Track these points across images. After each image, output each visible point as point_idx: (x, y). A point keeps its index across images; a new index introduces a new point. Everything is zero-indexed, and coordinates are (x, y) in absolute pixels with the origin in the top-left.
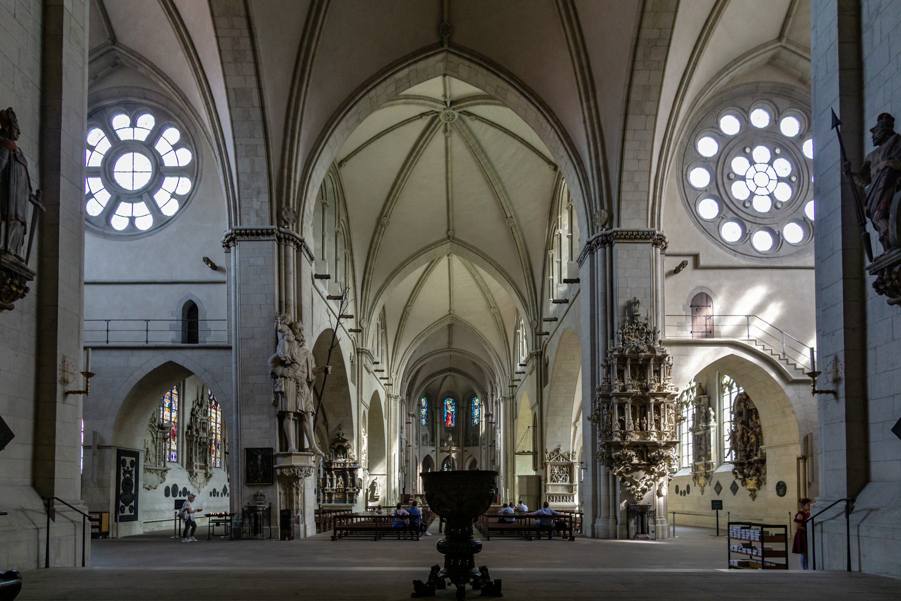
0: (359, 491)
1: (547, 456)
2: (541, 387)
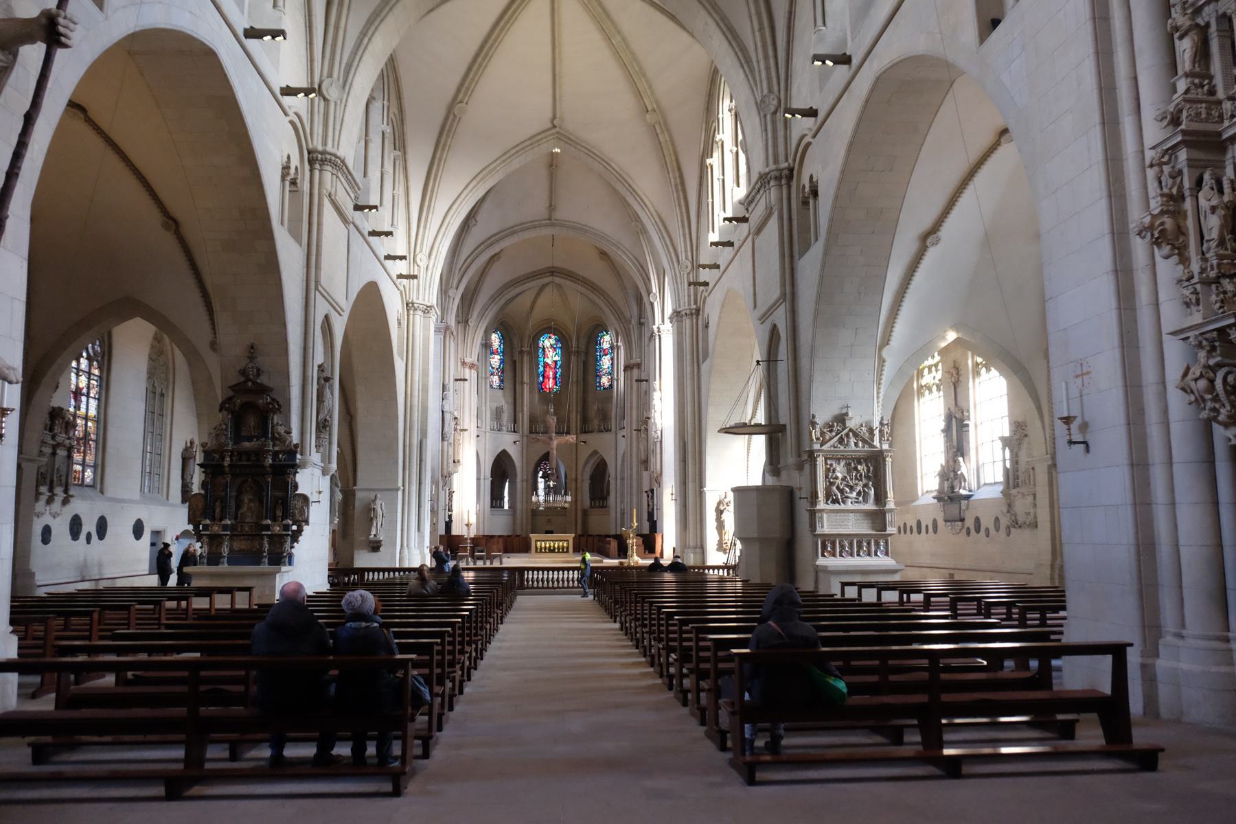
0: (300, 531)
1: (815, 434)
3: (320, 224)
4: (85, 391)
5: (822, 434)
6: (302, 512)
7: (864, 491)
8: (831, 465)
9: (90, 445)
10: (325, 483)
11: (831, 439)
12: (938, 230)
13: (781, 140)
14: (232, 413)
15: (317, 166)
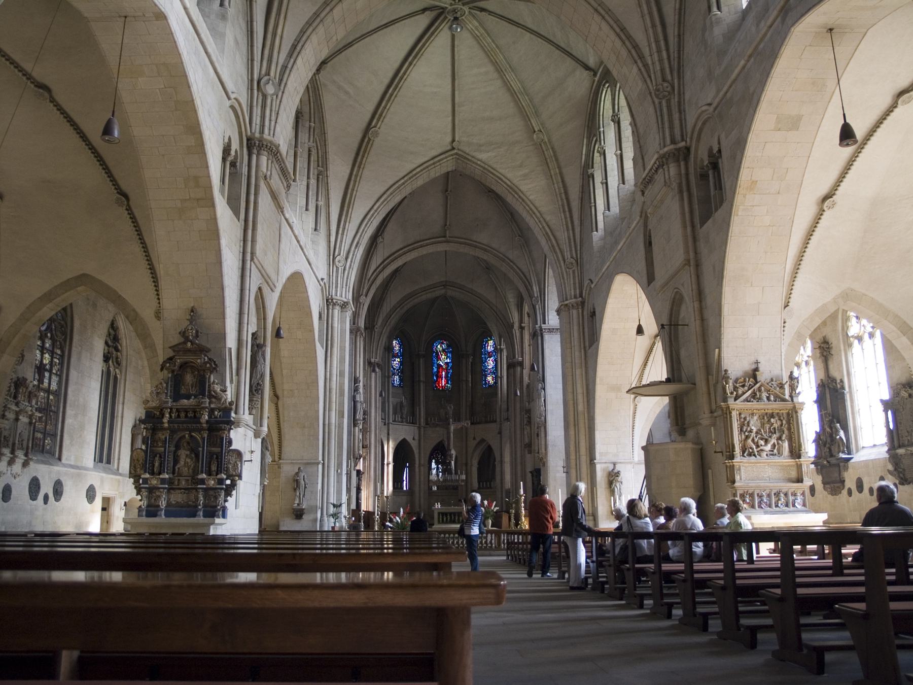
0: (233, 485)
1: (729, 387)
2: (693, 226)
3: (256, 203)
4: (48, 367)
5: (735, 388)
6: (235, 466)
7: (778, 444)
8: (745, 419)
9: (51, 416)
10: (257, 445)
11: (744, 393)
12: (834, 194)
13: (677, 123)
14: (173, 371)
15: (255, 151)
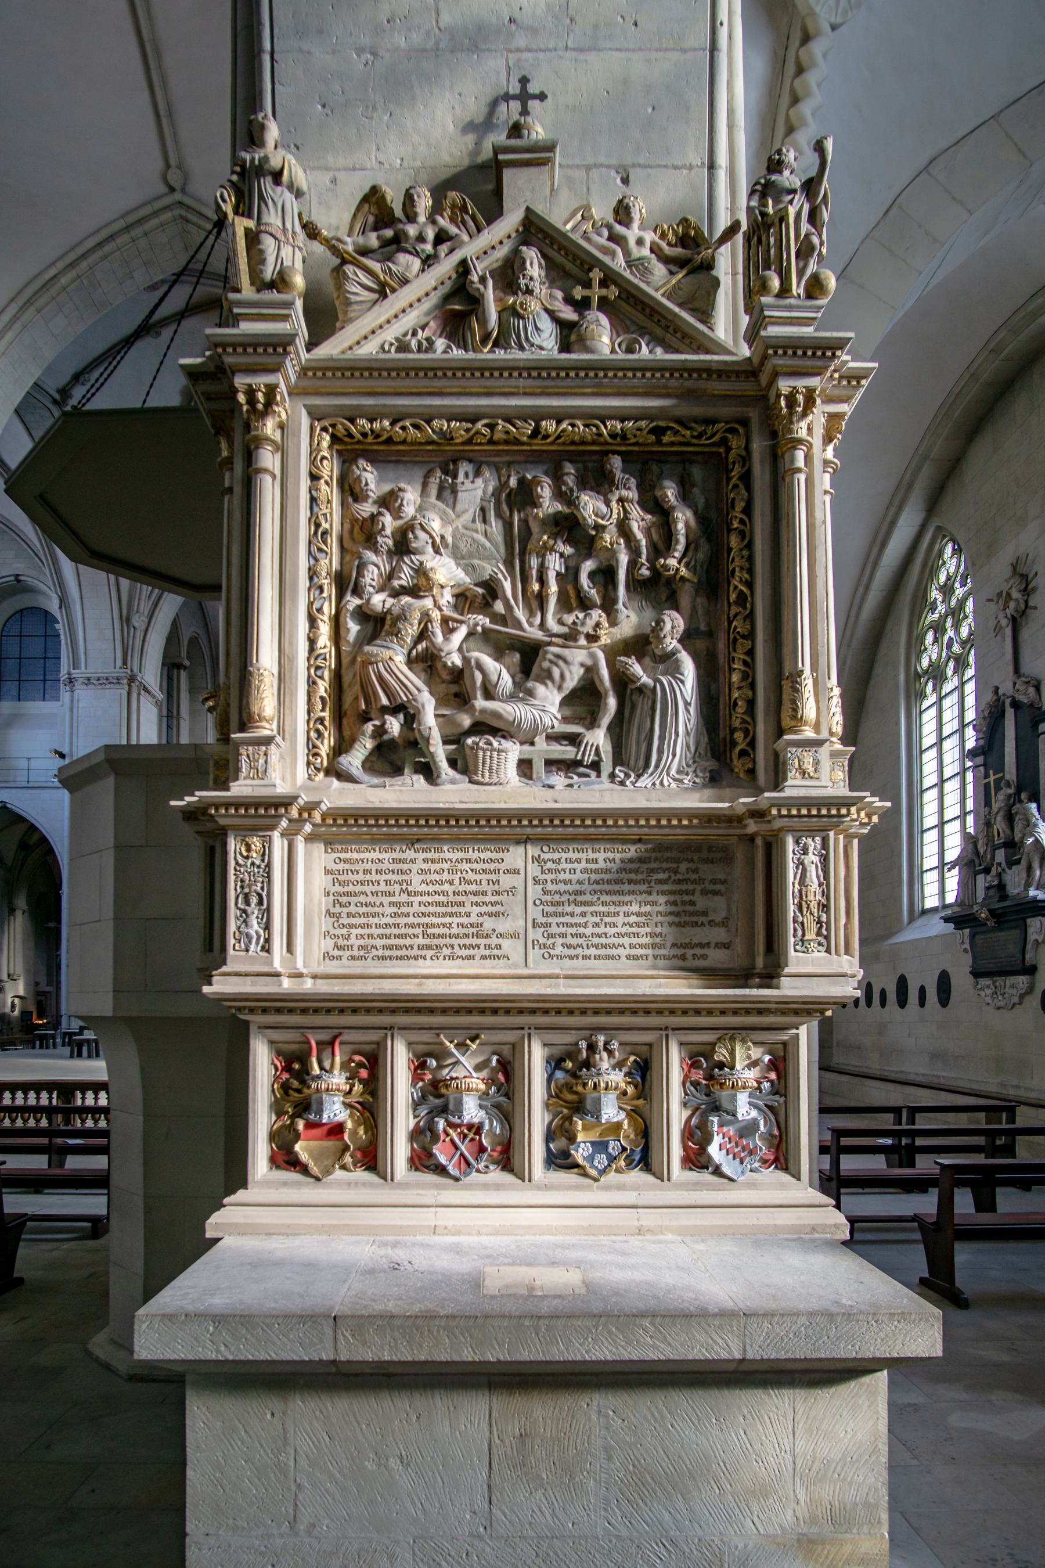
7: (623, 682)
8: (389, 501)
